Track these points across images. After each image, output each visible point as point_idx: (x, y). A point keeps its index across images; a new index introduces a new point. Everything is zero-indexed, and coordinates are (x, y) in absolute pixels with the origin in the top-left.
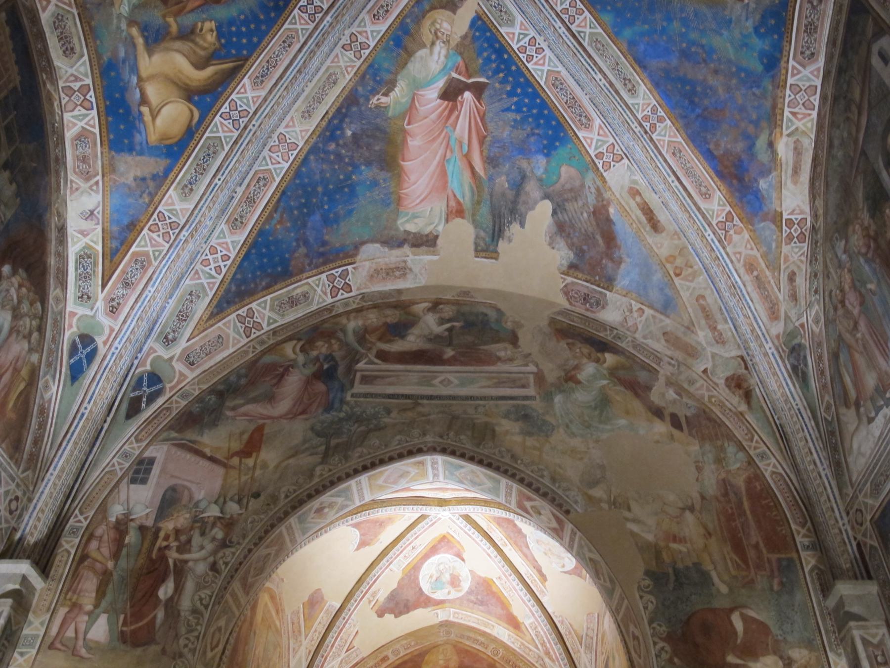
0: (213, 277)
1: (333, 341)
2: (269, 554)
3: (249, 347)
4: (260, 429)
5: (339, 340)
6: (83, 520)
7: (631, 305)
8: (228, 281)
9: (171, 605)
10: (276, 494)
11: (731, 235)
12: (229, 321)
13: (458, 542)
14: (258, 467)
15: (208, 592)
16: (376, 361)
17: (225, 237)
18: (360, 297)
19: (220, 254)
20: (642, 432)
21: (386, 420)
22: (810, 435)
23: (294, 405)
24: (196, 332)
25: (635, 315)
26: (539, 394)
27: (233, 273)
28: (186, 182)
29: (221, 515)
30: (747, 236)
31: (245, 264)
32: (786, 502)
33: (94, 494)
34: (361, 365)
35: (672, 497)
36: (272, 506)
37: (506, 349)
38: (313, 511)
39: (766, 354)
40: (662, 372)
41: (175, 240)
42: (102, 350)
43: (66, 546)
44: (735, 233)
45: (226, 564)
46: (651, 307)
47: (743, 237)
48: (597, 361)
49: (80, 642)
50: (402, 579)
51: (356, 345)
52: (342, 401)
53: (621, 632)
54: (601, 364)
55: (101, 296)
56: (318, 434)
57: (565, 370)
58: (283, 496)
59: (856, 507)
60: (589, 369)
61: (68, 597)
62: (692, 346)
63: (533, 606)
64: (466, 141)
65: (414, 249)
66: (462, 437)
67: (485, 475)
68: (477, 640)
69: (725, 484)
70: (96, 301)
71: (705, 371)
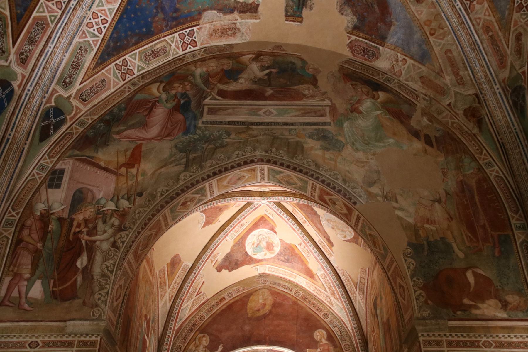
0: (97, 36)
1: (186, 83)
2: (152, 234)
3: (125, 88)
4: (138, 147)
5: (190, 82)
6: (15, 215)
7: (397, 57)
8: (107, 39)
9: (87, 271)
10: (154, 193)
11: (474, 5)
12: (110, 68)
13: (273, 221)
14: (140, 174)
16: (217, 97)
17: (103, 6)
18: (203, 50)
19: (100, 19)
20: (405, 148)
21: (228, 140)
22: (524, 150)
23: (162, 130)
24: (86, 77)
25: (400, 63)
26: (333, 121)
27: (110, 33)
29: (116, 209)
30: (486, 6)
31: (119, 26)
32: (505, 196)
33: (21, 196)
34: (207, 101)
36: (152, 202)
37: (309, 89)
38: (180, 204)
39: (494, 93)
40: (418, 105)
41: (66, 7)
42: (17, 91)
43: (5, 234)
44: (478, 3)
45: (123, 242)
46: (412, 58)
47: (483, 7)
48: (373, 97)
49: (23, 300)
50: (234, 246)
52: (196, 127)
53: (390, 282)
54: (376, 100)
56: (181, 151)
57: (351, 104)
58: (159, 195)
60: (367, 104)
61: (11, 269)
62: (441, 87)
63: (324, 263)
65: (241, 14)
66: (281, 152)
67: (297, 177)
68: (285, 286)
69: (463, 185)
70: (9, 54)
71: (449, 105)
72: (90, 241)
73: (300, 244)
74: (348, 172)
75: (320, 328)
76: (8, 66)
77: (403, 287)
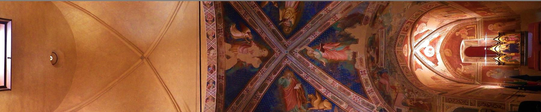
0: (360, 99)
28: (340, 103)
51: (375, 68)
52: (386, 69)
56: (392, 74)
64: (332, 47)
72: (416, 100)
74: (398, 23)
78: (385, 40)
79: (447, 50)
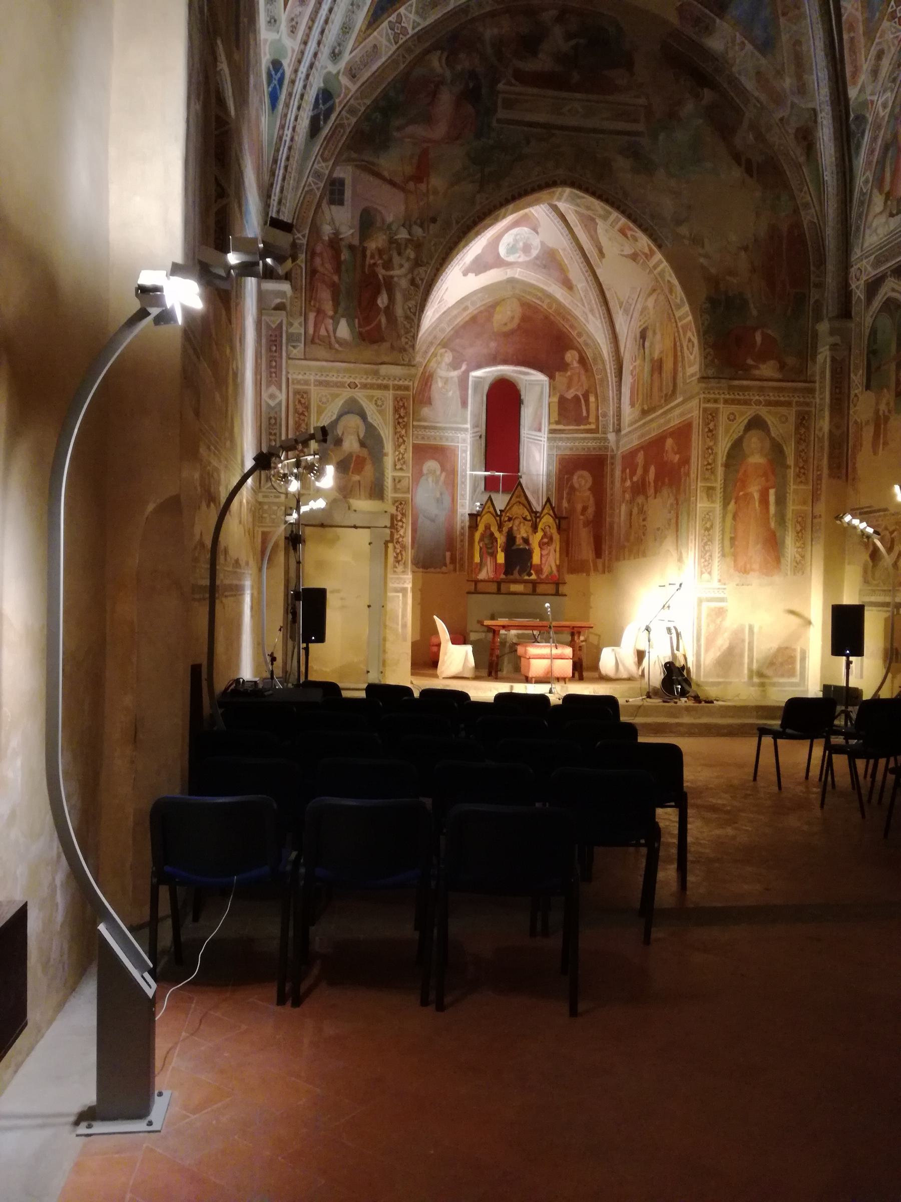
3: (398, 56)
4: (425, 153)
9: (389, 311)
15: (413, 302)
16: (513, 81)
24: (357, 44)
25: (737, 48)
34: (501, 86)
35: (733, 238)
45: (422, 280)
46: (752, 42)
55: (284, 18)
59: (858, 266)
67: (602, 207)
70: (281, 23)
71: (782, 119)
73: (564, 250)
75: (572, 349)
76: (280, 40)
77: (693, 342)
78: (602, 131)
79: (518, 311)
